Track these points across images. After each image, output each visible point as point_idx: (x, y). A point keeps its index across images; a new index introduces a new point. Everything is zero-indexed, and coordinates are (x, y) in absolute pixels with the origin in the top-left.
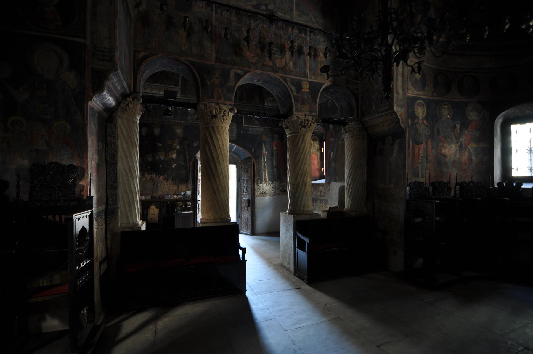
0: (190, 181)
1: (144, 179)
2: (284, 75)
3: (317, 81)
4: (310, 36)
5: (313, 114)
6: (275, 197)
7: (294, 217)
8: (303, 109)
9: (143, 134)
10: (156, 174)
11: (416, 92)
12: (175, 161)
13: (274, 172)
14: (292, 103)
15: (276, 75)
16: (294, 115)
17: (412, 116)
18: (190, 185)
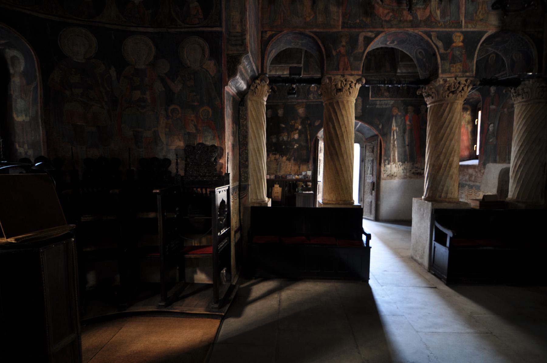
0: (311, 161)
2: (428, 29)
5: (468, 74)
6: (406, 180)
7: (432, 205)
8: (453, 69)
12: (297, 141)
13: (405, 151)
14: (437, 64)
15: (416, 31)
16: (439, 79)
18: (311, 165)
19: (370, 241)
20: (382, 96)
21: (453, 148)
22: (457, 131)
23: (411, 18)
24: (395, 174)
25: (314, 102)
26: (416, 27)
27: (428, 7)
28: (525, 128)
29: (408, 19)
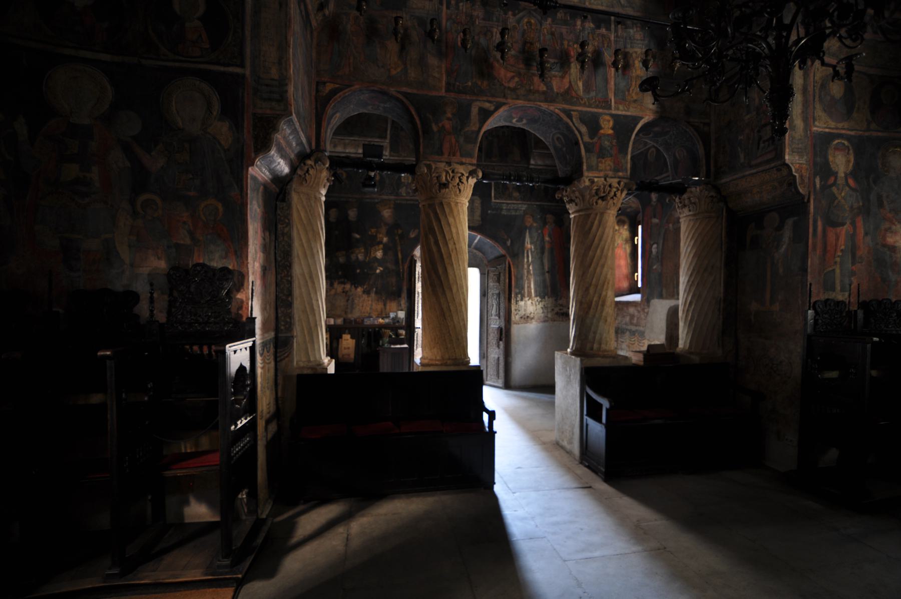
0: (404, 295)
1: (333, 292)
2: (567, 107)
3: (629, 113)
4: (616, 31)
5: (620, 174)
6: (547, 324)
7: (581, 361)
8: (601, 166)
9: (332, 219)
10: (352, 284)
11: (833, 124)
12: (380, 262)
13: (544, 281)
15: (552, 108)
16: (584, 178)
17: (824, 170)
18: (404, 302)
19: (495, 422)
20: (510, 197)
21: (606, 278)
22: (610, 254)
23: (545, 89)
24: (532, 316)
25: (407, 200)
26: (551, 102)
27: (567, 76)
28: (694, 251)
29: (541, 89)
